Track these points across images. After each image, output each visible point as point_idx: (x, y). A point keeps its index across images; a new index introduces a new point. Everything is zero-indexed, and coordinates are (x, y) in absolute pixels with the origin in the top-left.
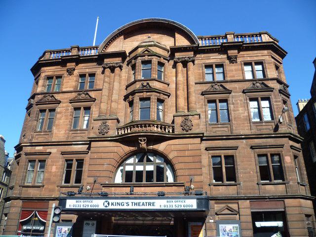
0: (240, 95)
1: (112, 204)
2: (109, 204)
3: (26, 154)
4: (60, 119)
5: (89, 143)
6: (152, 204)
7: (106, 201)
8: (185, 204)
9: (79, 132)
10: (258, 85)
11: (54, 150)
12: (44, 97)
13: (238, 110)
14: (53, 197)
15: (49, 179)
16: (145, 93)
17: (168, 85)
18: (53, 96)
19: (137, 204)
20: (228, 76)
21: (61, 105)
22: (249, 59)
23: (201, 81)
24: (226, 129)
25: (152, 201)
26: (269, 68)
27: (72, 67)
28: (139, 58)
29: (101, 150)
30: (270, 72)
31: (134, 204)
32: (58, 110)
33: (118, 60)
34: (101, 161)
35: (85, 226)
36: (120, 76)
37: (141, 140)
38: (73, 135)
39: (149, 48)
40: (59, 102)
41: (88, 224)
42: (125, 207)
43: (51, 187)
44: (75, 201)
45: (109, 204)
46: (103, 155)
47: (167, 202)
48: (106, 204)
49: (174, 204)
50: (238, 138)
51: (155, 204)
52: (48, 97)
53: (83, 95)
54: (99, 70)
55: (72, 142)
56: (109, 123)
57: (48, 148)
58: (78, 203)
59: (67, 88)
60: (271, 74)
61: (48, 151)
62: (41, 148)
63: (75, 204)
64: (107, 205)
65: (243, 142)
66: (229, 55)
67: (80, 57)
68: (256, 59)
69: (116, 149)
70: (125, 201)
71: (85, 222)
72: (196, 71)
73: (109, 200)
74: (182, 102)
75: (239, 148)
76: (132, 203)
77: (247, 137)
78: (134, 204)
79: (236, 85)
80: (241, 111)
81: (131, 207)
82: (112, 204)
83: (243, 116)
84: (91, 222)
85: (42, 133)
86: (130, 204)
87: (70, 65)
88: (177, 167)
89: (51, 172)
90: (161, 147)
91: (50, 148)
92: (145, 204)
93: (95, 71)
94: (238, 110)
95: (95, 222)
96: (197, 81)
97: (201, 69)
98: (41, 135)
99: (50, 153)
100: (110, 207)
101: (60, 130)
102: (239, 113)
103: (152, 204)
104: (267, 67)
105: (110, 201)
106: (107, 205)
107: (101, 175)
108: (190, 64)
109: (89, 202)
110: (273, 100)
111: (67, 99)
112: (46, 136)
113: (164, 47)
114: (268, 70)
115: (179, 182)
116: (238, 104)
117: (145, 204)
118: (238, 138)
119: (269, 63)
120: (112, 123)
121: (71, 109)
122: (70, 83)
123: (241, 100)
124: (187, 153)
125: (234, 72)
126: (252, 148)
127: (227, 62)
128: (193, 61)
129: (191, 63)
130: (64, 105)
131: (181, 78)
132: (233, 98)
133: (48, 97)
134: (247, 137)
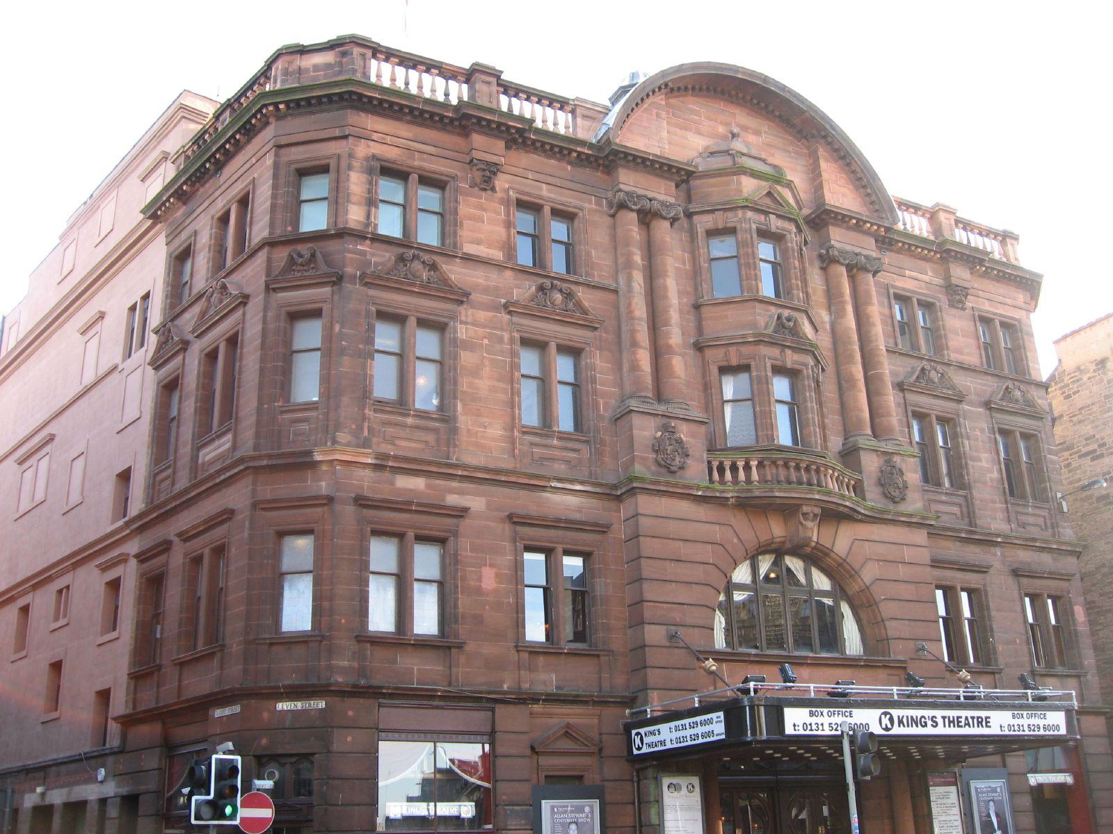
1: (901, 722)
2: (891, 720)
3: (361, 502)
4: (475, 372)
5: (619, 492)
6: (984, 723)
7: (886, 714)
8: (1046, 722)
12: (401, 259)
13: (980, 460)
14: (505, 687)
15: (479, 619)
16: (788, 352)
18: (433, 267)
19: (953, 722)
21: (466, 313)
24: (956, 510)
25: (983, 714)
28: (750, 214)
29: (672, 527)
31: (947, 720)
33: (661, 192)
34: (684, 572)
35: (665, 788)
37: (805, 514)
39: (779, 188)
40: (460, 297)
41: (676, 787)
42: (929, 730)
43: (488, 649)
44: (806, 711)
45: (891, 720)
46: (685, 550)
47: (1014, 717)
48: (886, 721)
49: (1025, 722)
50: (987, 542)
51: (992, 722)
52: (417, 265)
53: (558, 297)
54: (588, 207)
55: (572, 481)
56: (684, 432)
57: (451, 491)
58: (814, 720)
59: (478, 242)
61: (452, 500)
62: (417, 484)
63: (809, 720)
64: (889, 726)
65: (995, 555)
66: (954, 281)
69: (717, 533)
70: (928, 713)
71: (666, 781)
73: (892, 711)
75: (992, 571)
76: (944, 718)
77: (1008, 542)
78: (947, 720)
80: (984, 464)
81: (941, 730)
82: (901, 722)
83: (991, 480)
84: (682, 781)
85: (410, 420)
86: (940, 721)
87: (486, 147)
89: (479, 591)
90: (842, 541)
91: (461, 492)
92: (970, 720)
93: (579, 203)
94: (980, 460)
95: (695, 781)
98: (404, 426)
99: (462, 513)
100: (897, 730)
101: (485, 420)
103: (984, 723)
105: (896, 713)
106: (889, 726)
107: (689, 621)
109: (844, 715)
111: (486, 290)
112: (430, 438)
115: (892, 658)
116: (977, 439)
117: (970, 720)
118: (987, 542)
120: (693, 435)
122: (486, 227)
123: (982, 430)
124: (902, 572)
125: (961, 339)
126: (1016, 573)
127: (942, 301)
130: (482, 315)
131: (850, 321)
133: (417, 265)
134: (1008, 542)
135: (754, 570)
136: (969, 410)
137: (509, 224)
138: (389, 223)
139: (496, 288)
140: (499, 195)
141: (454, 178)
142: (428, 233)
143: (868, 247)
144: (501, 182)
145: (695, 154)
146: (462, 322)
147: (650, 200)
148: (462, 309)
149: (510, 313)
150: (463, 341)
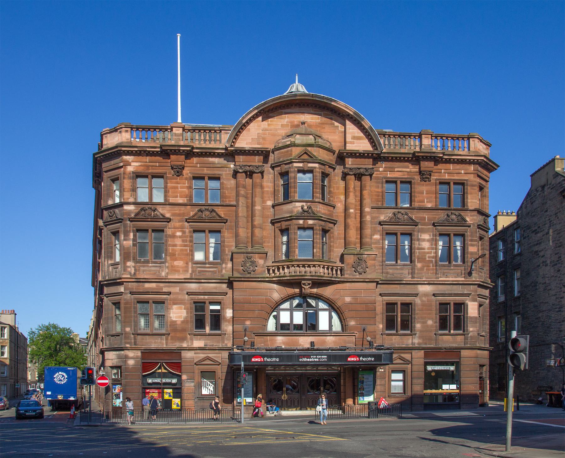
0: (429, 228)
9: (207, 265)
10: (453, 217)
11: (175, 289)
17: (334, 207)
20: (416, 199)
22: (447, 177)
23: (380, 204)
26: (471, 194)
27: (180, 163)
30: (472, 199)
32: (169, 231)
36: (262, 187)
38: (199, 269)
40: (169, 220)
53: (207, 213)
60: (472, 202)
62: (154, 285)
67: (193, 148)
68: (456, 177)
72: (374, 189)
74: (353, 235)
79: (426, 215)
88: (347, 314)
90: (327, 291)
96: (375, 205)
97: (380, 185)
102: (425, 253)
104: (469, 192)
108: (366, 179)
110: (468, 238)
111: (179, 215)
113: (327, 145)
114: (469, 196)
119: (472, 185)
121: (190, 232)
127: (418, 178)
128: (371, 175)
129: (369, 177)
131: (353, 199)
132: (418, 232)
135: (291, 305)
136: (422, 228)
137: (190, 187)
138: (143, 196)
139: (184, 213)
140: (185, 176)
141: (166, 173)
142: (158, 197)
143: (368, 163)
144: (186, 171)
145: (280, 137)
146: (169, 228)
147: (249, 166)
148: (169, 224)
149: (189, 222)
150: (169, 235)
